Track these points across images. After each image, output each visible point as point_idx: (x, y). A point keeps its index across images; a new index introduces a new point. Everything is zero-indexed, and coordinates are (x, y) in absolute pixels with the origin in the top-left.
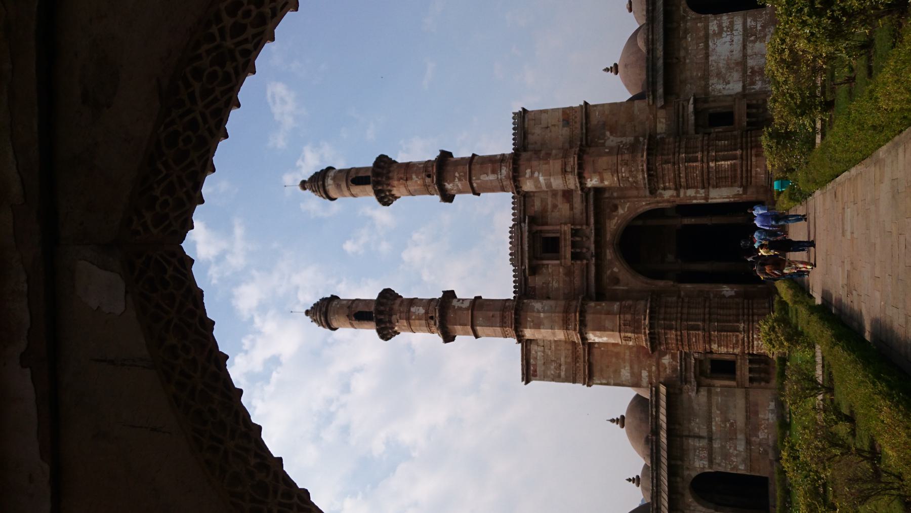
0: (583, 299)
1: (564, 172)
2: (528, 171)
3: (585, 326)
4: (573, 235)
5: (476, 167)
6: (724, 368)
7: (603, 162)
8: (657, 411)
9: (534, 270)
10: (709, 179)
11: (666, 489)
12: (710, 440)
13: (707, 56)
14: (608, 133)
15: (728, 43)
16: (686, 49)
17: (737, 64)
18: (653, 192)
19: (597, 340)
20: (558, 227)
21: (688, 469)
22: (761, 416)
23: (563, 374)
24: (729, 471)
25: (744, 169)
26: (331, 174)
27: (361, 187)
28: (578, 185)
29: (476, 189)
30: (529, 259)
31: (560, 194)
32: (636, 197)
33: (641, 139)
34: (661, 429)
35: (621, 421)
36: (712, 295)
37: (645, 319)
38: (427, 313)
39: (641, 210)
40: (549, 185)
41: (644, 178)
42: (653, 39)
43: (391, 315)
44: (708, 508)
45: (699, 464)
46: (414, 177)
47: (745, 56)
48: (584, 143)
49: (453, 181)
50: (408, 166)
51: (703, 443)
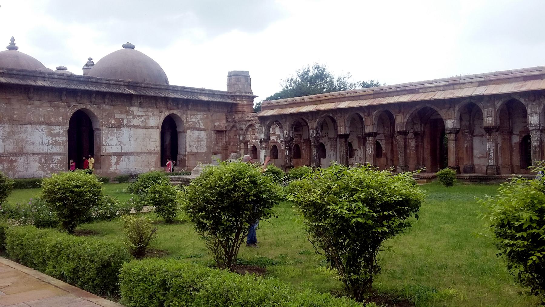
13: (31, 123)
15: (41, 141)
16: (41, 106)
17: (21, 149)
42: (53, 78)
47: (28, 155)
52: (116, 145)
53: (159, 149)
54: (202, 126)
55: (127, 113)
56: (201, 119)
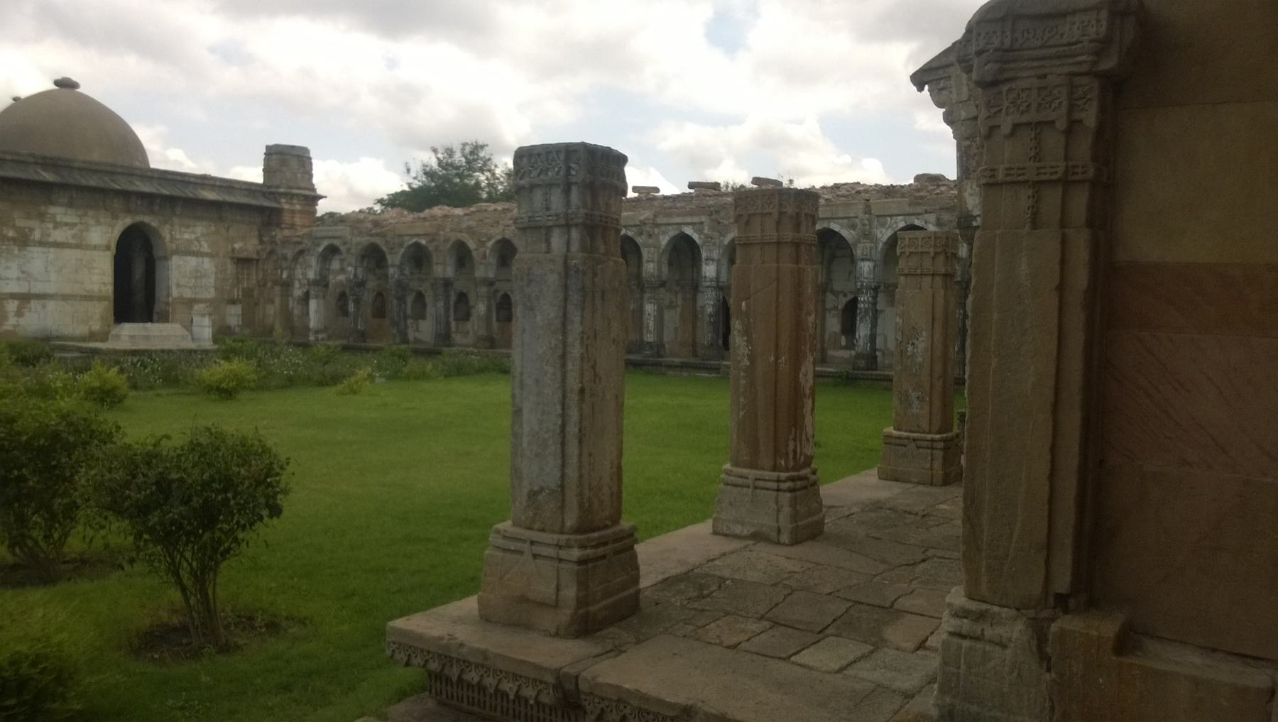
52: (18, 279)
53: (110, 289)
54: (205, 248)
55: (42, 217)
56: (203, 235)
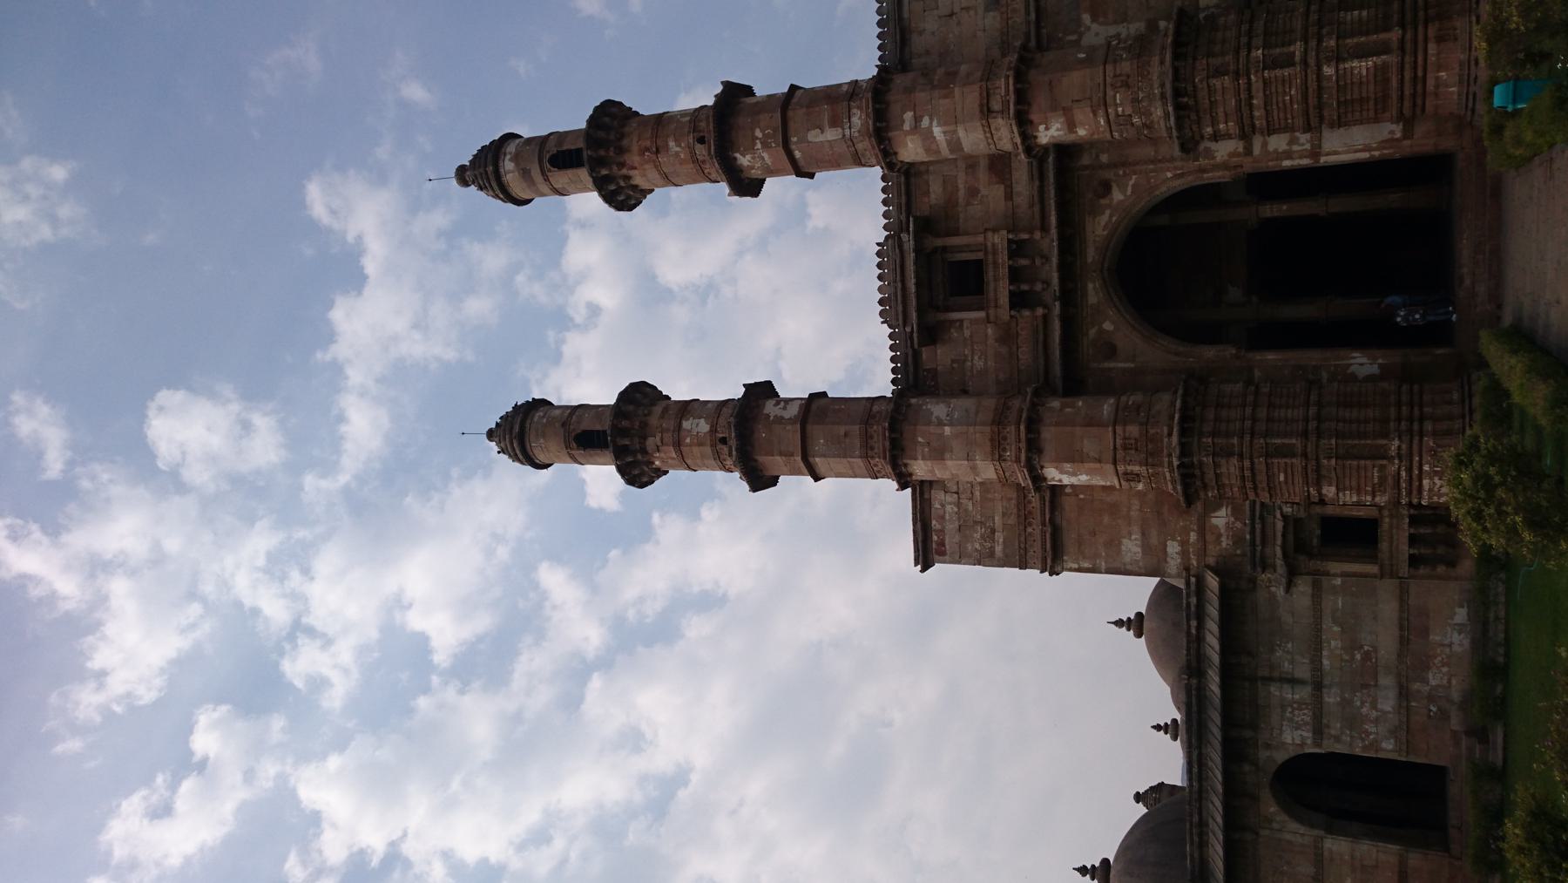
0: (1036, 393)
1: (986, 112)
2: (909, 115)
3: (1040, 451)
4: (1013, 254)
5: (797, 115)
6: (1353, 535)
7: (1074, 81)
8: (1200, 627)
9: (931, 333)
10: (1320, 107)
11: (1220, 788)
12: (1318, 686)
14: (1086, 18)
18: (1189, 146)
19: (1066, 480)
20: (980, 239)
21: (1268, 746)
22: (1435, 638)
23: (999, 549)
24: (1358, 751)
25: (1408, 75)
26: (511, 148)
27: (570, 172)
28: (1018, 141)
29: (802, 163)
30: (920, 311)
31: (983, 163)
32: (1152, 162)
33: (1162, 24)
34: (1215, 656)
35: (1136, 624)
36: (1325, 375)
37: (1170, 435)
38: (713, 430)
39: (1163, 191)
40: (955, 145)
41: (1167, 115)
43: (645, 438)
44: (1312, 826)
45: (1292, 736)
46: (672, 144)
48: (1033, 43)
49: (751, 148)
50: (660, 120)
51: (1303, 693)
